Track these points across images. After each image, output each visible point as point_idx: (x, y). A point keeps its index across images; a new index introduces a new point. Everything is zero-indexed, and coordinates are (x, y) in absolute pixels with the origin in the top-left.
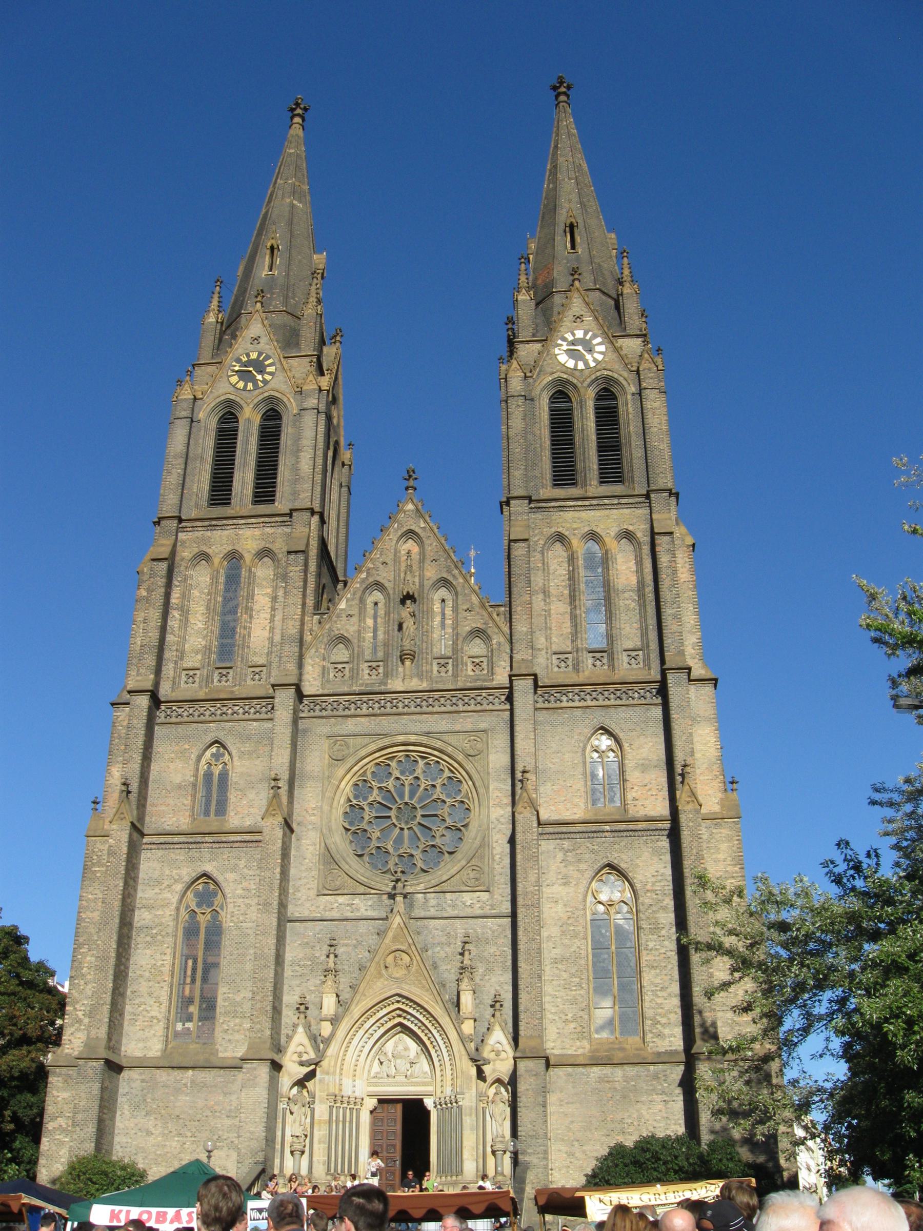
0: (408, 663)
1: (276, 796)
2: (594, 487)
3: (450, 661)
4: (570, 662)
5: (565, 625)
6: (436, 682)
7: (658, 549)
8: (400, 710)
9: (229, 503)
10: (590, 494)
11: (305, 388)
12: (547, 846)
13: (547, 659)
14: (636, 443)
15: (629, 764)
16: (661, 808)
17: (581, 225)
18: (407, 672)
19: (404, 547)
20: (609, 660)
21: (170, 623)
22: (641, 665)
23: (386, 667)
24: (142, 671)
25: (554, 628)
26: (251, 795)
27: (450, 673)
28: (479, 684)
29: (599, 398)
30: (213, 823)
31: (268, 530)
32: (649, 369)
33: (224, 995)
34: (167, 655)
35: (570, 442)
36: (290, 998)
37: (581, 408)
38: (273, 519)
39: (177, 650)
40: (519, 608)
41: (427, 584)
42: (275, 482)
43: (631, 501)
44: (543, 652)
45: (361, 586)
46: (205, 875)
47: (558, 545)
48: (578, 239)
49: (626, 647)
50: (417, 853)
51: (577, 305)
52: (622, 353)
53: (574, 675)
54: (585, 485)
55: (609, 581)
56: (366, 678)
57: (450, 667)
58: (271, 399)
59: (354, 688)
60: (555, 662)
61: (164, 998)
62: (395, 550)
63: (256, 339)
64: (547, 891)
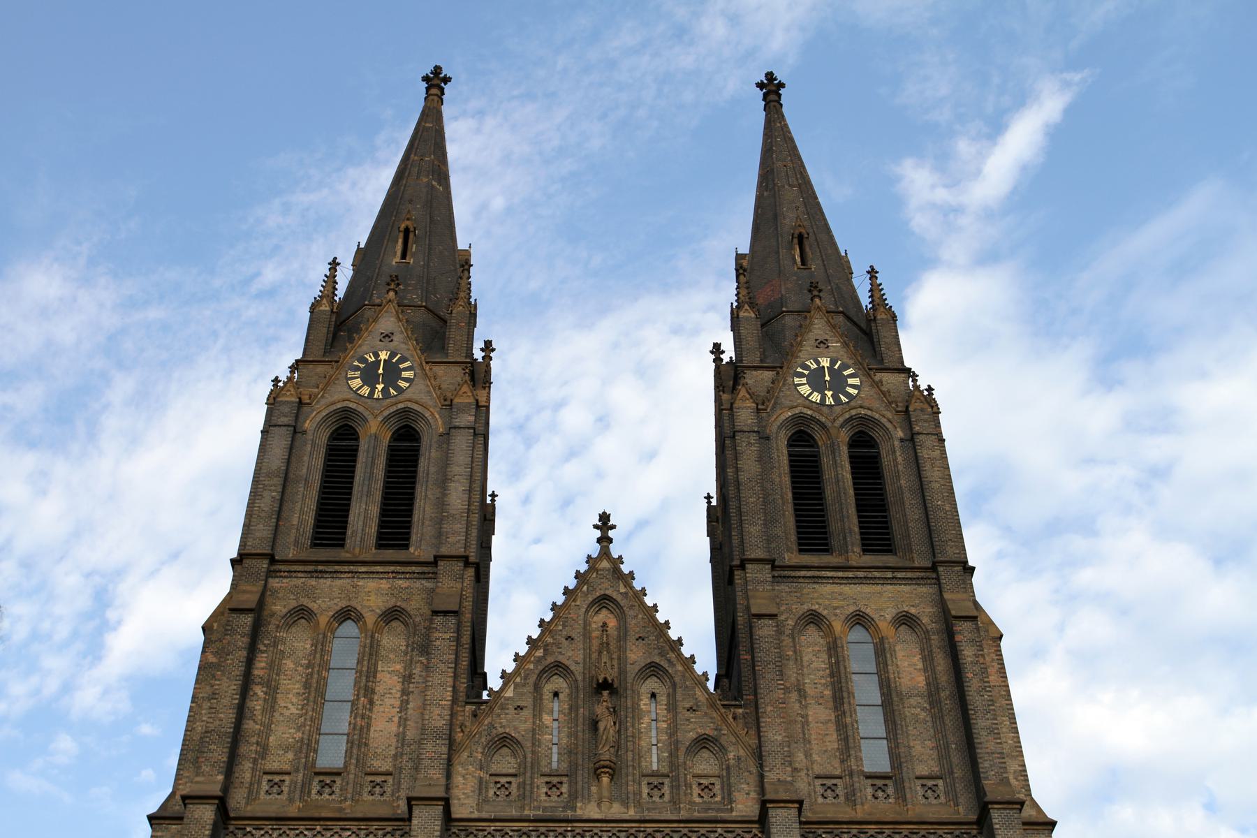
0: (605, 780)
2: (856, 556)
3: (667, 781)
4: (840, 791)
5: (828, 738)
6: (648, 809)
7: (958, 638)
9: (342, 546)
11: (456, 401)
13: (810, 785)
14: (910, 501)
17: (812, 238)
18: (606, 793)
19: (595, 619)
20: (896, 790)
21: (250, 704)
22: (943, 799)
24: (205, 768)
25: (814, 742)
27: (667, 797)
28: (711, 814)
29: (853, 444)
31: (401, 582)
32: (922, 410)
34: (243, 749)
35: (819, 495)
37: (833, 452)
38: (408, 569)
39: (258, 743)
40: (769, 708)
41: (632, 670)
42: (410, 522)
43: (909, 575)
44: (803, 773)
45: (536, 667)
47: (812, 629)
49: (918, 774)
51: (819, 328)
52: (884, 389)
53: (849, 809)
54: (844, 550)
55: (888, 679)
56: (544, 800)
57: (666, 790)
58: (406, 411)
59: (526, 812)
60: (820, 790)
62: (585, 621)
63: (388, 336)
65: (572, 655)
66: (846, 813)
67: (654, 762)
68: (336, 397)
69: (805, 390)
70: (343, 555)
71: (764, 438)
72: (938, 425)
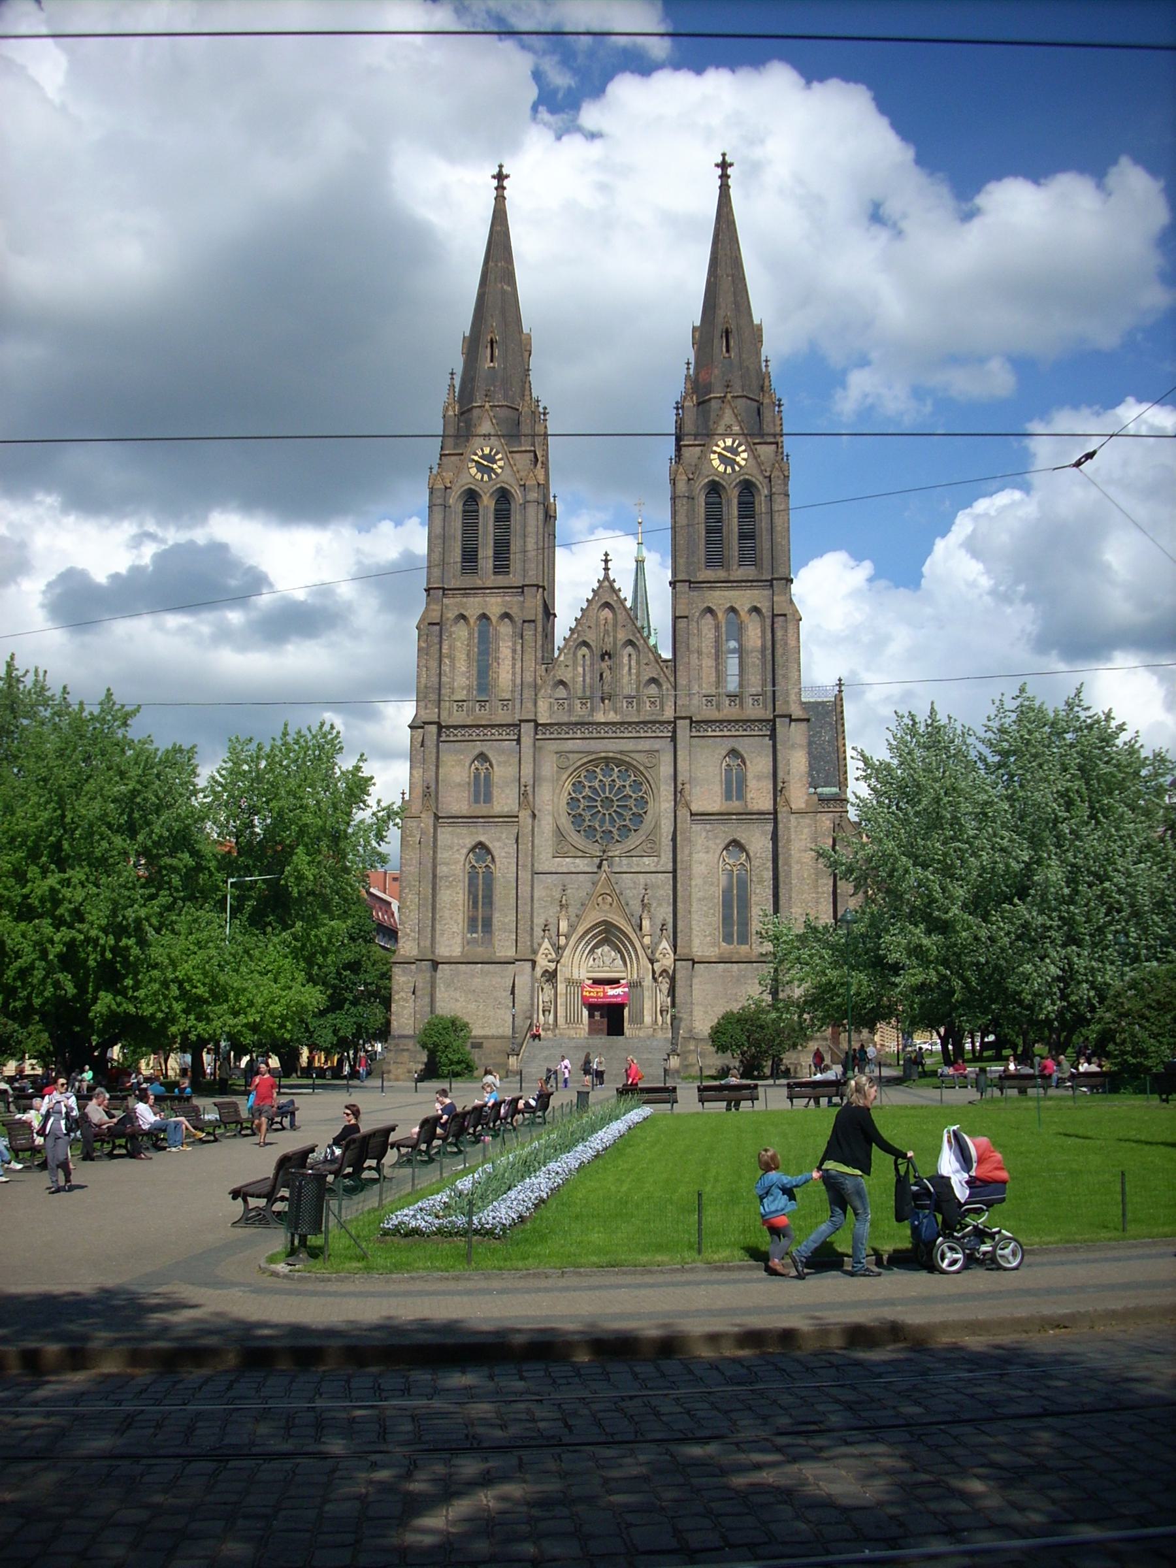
1: (525, 794)
8: (603, 735)
10: (732, 578)
12: (697, 828)
14: (765, 536)
15: (750, 775)
16: (766, 804)
23: (592, 703)
26: (507, 791)
30: (482, 809)
33: (497, 918)
34: (443, 691)
35: (719, 531)
36: (539, 921)
41: (619, 644)
46: (481, 845)
48: (732, 344)
50: (614, 830)
51: (728, 417)
54: (728, 570)
56: (580, 712)
61: (460, 921)
64: (695, 856)
65: (590, 637)
66: (716, 715)
67: (629, 690)
68: (463, 483)
69: (716, 463)
70: (479, 583)
71: (691, 498)
72: (786, 485)
